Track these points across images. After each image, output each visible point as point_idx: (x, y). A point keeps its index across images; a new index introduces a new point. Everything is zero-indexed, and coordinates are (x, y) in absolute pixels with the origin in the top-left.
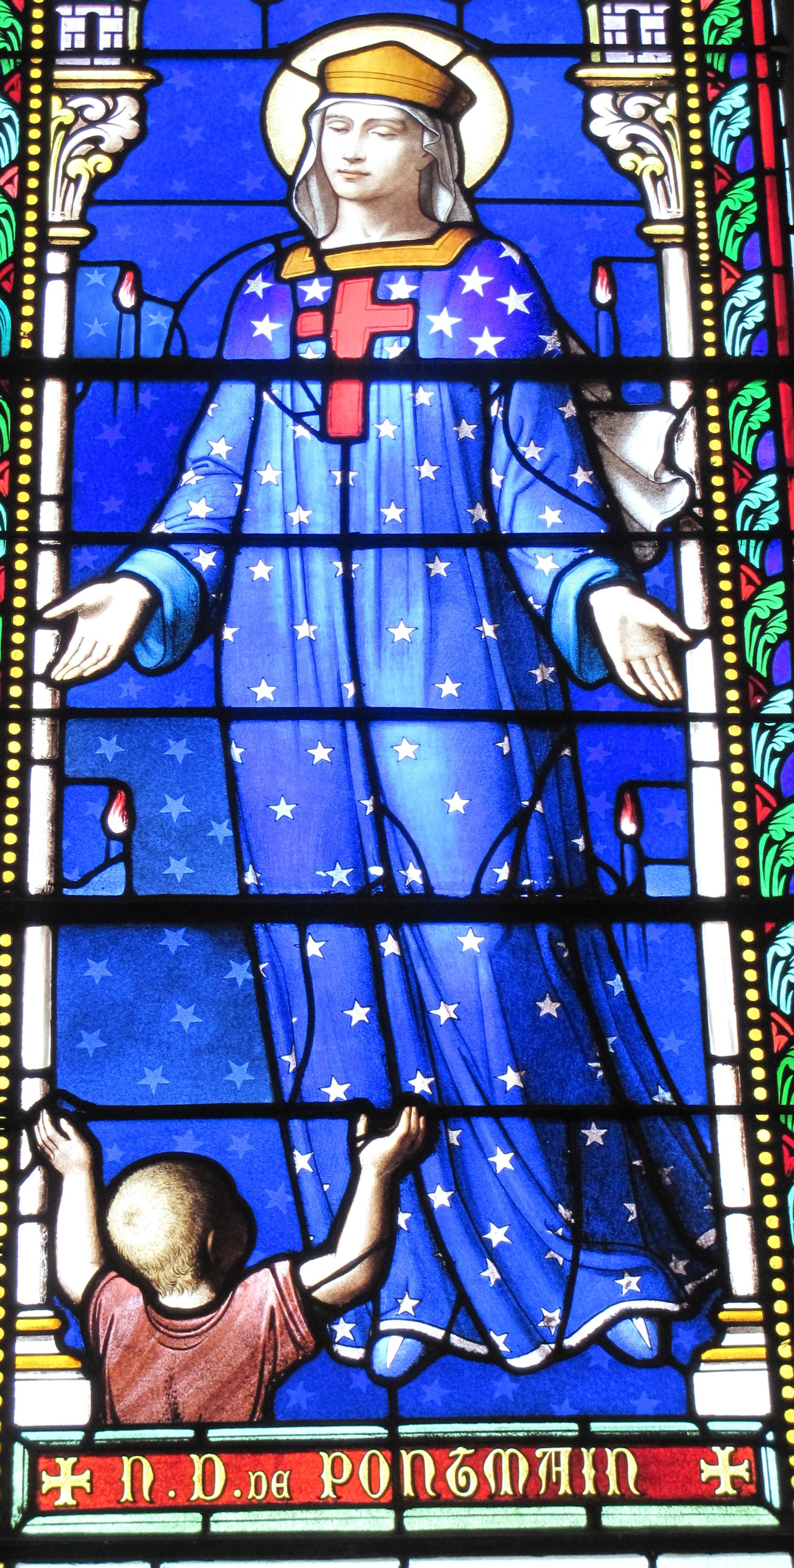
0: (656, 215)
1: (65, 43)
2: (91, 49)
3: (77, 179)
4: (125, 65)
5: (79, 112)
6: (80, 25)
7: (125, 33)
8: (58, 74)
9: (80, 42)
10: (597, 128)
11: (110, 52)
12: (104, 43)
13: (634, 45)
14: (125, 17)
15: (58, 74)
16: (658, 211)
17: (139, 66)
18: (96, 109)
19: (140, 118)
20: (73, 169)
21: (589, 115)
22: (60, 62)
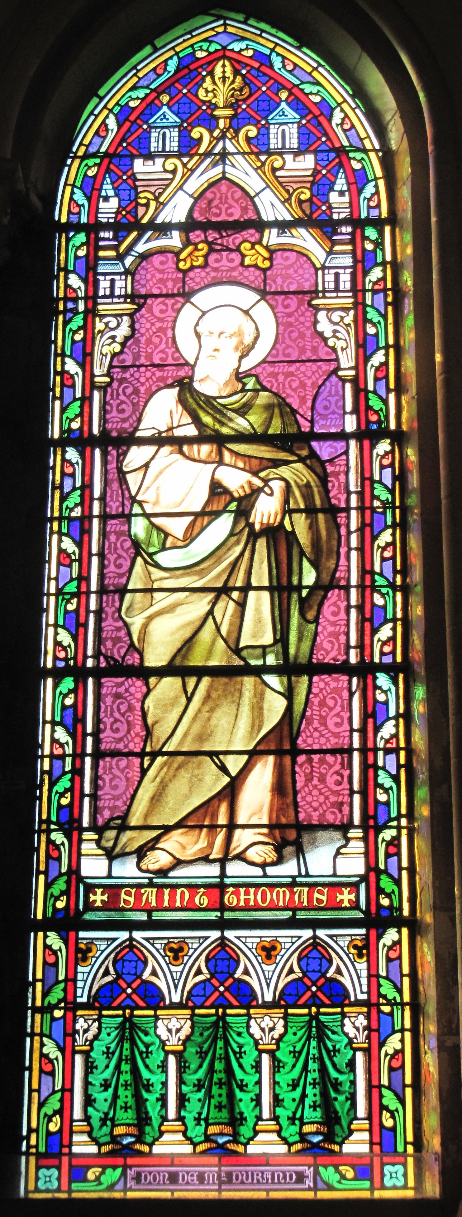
0: (342, 366)
1: (101, 293)
2: (112, 295)
3: (106, 355)
4: (125, 302)
5: (107, 324)
6: (107, 284)
7: (126, 288)
8: (100, 307)
9: (108, 292)
10: (319, 328)
11: (119, 297)
12: (117, 292)
13: (337, 289)
14: (126, 280)
15: (100, 307)
16: (344, 364)
17: (132, 302)
18: (113, 323)
19: (132, 326)
20: (106, 350)
21: (316, 322)
22: (99, 300)
